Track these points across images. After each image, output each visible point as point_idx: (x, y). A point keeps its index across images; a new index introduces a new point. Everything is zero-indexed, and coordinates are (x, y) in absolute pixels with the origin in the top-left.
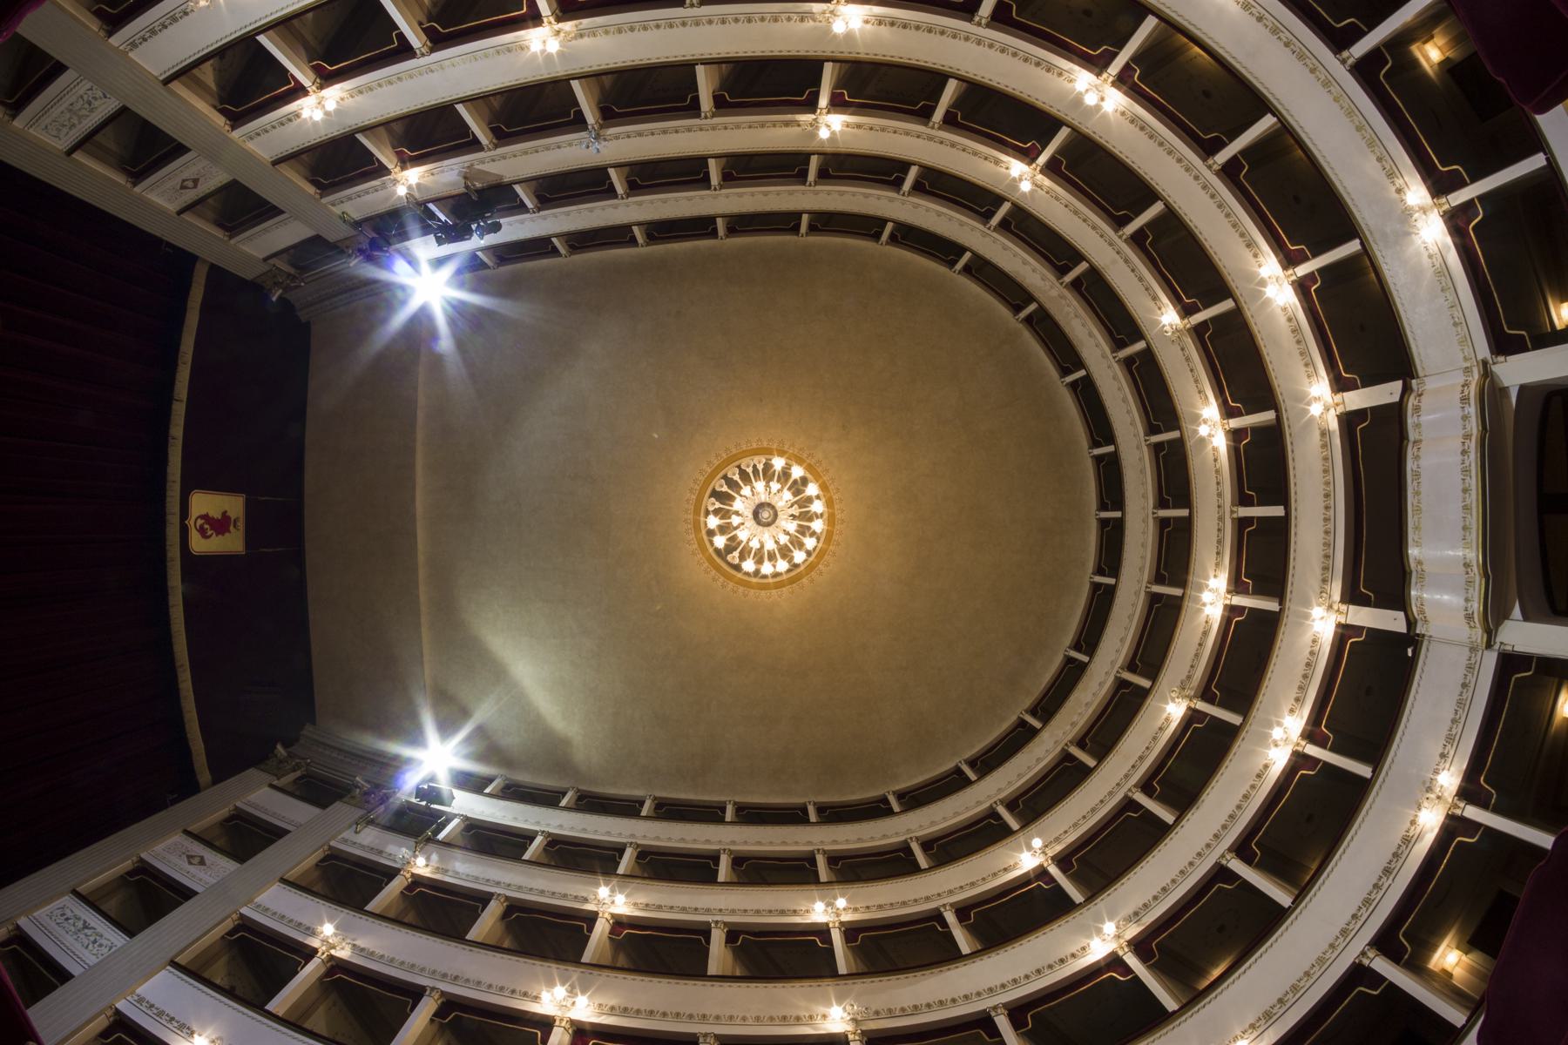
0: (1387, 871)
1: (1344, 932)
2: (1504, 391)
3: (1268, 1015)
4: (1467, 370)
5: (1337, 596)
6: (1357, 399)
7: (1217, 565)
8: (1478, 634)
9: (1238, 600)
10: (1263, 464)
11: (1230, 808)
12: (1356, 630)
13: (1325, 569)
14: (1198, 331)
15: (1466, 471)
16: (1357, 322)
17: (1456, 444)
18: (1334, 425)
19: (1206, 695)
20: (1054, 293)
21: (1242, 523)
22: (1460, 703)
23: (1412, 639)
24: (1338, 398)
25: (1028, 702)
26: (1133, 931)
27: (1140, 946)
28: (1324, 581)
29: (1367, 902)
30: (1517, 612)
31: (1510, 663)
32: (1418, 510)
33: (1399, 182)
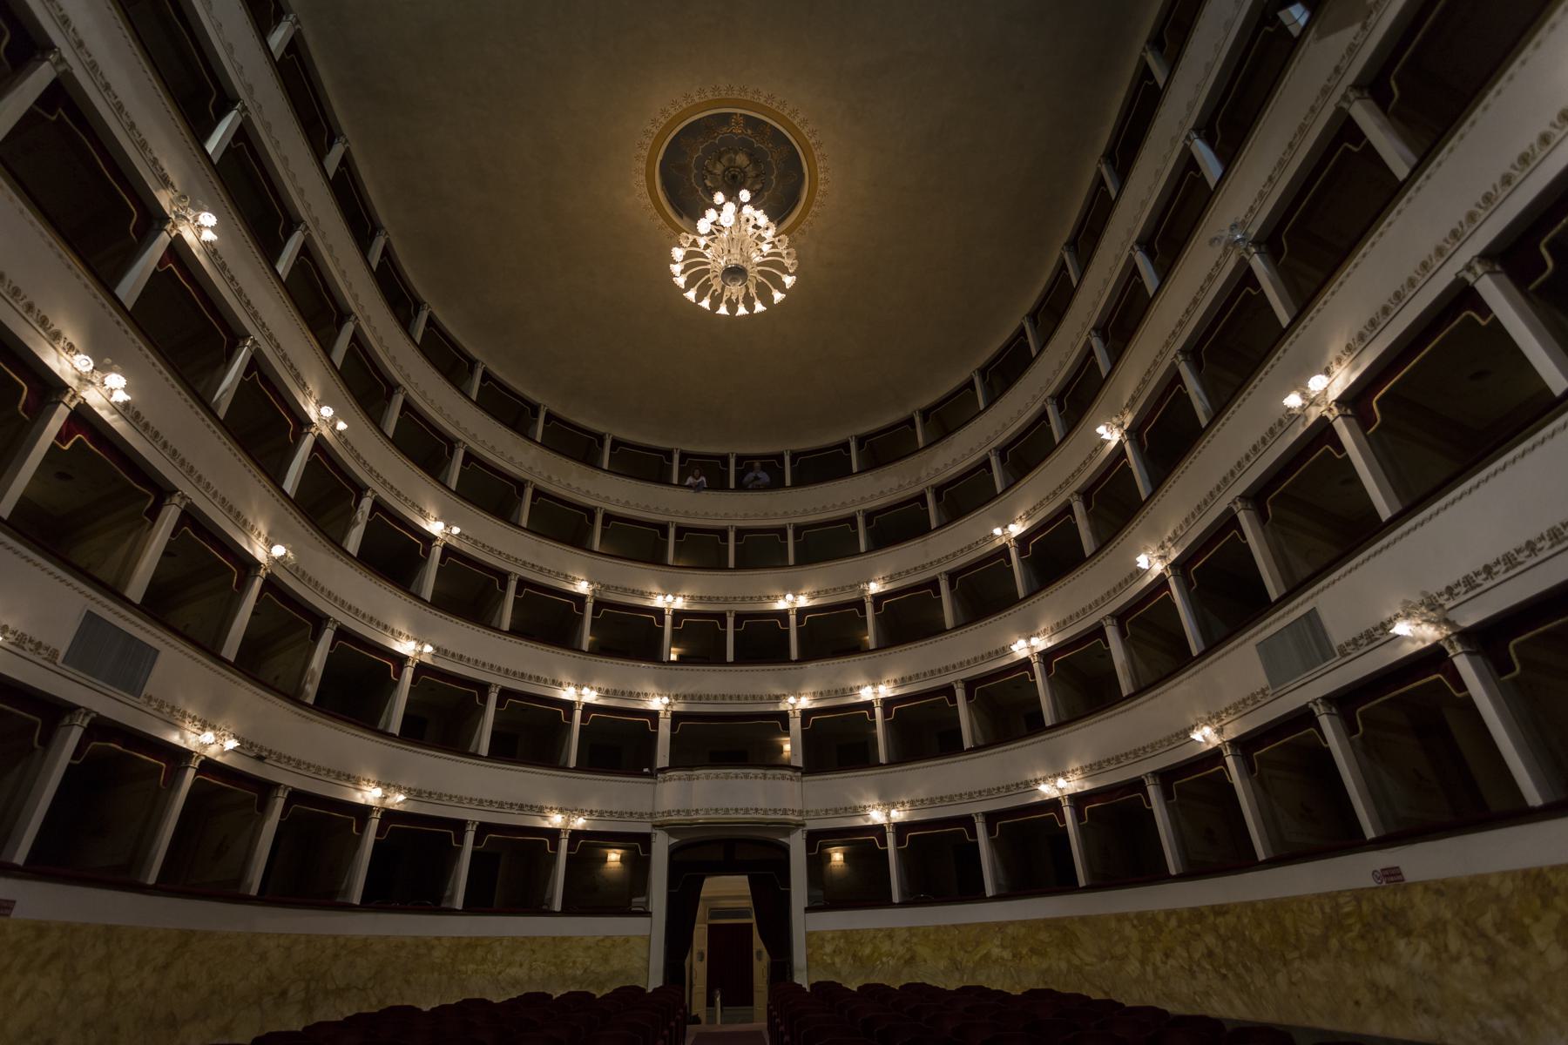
2: (788, 835)
4: (801, 813)
5: (675, 708)
6: (795, 725)
7: (692, 598)
9: (668, 619)
10: (763, 641)
11: (528, 669)
12: (656, 725)
13: (693, 697)
14: (860, 604)
15: (747, 811)
16: (839, 742)
17: (762, 804)
18: (782, 707)
19: (599, 604)
21: (721, 617)
22: (621, 814)
24: (798, 714)
28: (685, 697)
30: (674, 841)
31: (645, 840)
32: (727, 777)
33: (907, 806)
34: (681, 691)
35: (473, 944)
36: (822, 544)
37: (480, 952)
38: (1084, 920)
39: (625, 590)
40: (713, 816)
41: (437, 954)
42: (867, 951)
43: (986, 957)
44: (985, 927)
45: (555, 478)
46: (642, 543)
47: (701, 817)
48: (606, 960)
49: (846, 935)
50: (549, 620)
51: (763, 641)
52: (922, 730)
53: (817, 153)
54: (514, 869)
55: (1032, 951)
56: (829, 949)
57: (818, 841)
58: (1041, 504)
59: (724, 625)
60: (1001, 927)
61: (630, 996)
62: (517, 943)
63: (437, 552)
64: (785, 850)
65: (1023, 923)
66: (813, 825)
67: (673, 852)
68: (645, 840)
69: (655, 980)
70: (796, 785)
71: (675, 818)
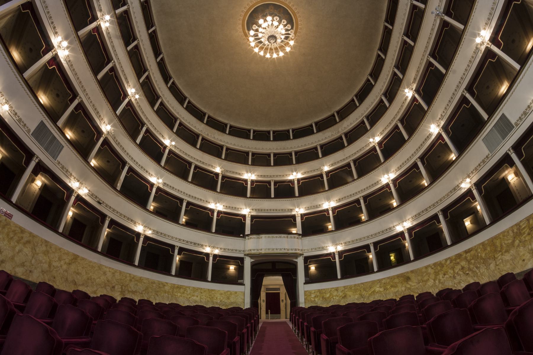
0: (195, 244)
1: (180, 240)
3: (157, 232)
5: (252, 214)
6: (299, 220)
7: (258, 176)
8: (247, 252)
9: (249, 183)
10: (285, 191)
11: (197, 196)
12: (245, 220)
13: (259, 210)
14: (321, 176)
15: (281, 249)
16: (314, 225)
18: (293, 213)
19: (224, 177)
20: (340, 130)
21: (269, 183)
22: (232, 250)
23: (244, 236)
24: (299, 215)
25: (212, 115)
26: (161, 186)
27: (159, 189)
28: (256, 210)
29: (187, 242)
30: (253, 260)
31: (242, 260)
32: (273, 237)
34: (254, 208)
35: (179, 287)
36: (305, 156)
37: (182, 290)
38: (412, 272)
39: (233, 172)
40: (267, 252)
41: (167, 288)
42: (328, 295)
43: (374, 292)
44: (373, 282)
45: (210, 134)
46: (238, 157)
47: (263, 252)
48: (228, 298)
49: (320, 291)
50: (205, 180)
51: (285, 191)
52: (346, 217)
53: (297, 15)
54: (194, 266)
55: (392, 286)
56: (313, 296)
57: (308, 260)
58: (386, 128)
59: (270, 185)
60: (380, 281)
61: (236, 311)
62: (195, 289)
63: (167, 151)
64: (295, 265)
65: (388, 278)
66: (306, 254)
67: (253, 265)
68: (242, 260)
69: (247, 305)
70: (300, 240)
71: (253, 252)
